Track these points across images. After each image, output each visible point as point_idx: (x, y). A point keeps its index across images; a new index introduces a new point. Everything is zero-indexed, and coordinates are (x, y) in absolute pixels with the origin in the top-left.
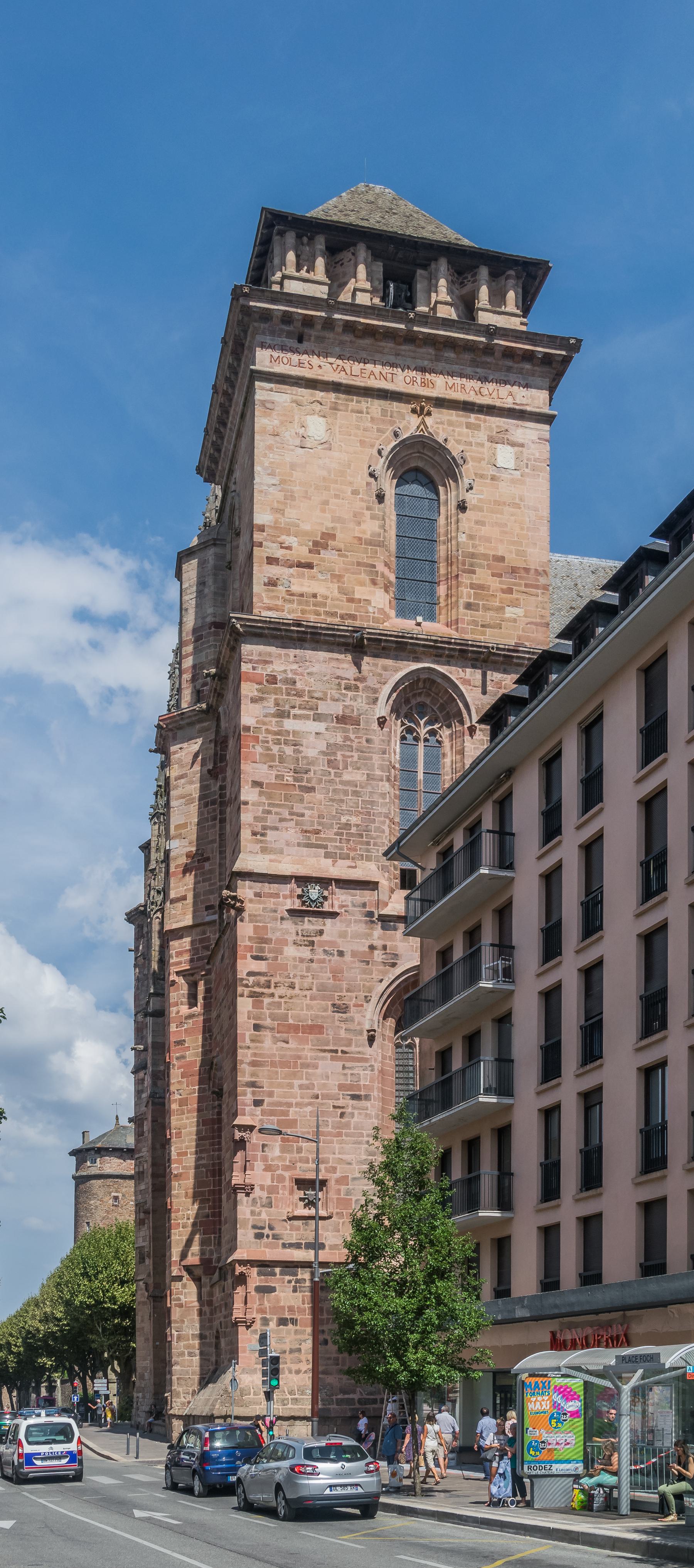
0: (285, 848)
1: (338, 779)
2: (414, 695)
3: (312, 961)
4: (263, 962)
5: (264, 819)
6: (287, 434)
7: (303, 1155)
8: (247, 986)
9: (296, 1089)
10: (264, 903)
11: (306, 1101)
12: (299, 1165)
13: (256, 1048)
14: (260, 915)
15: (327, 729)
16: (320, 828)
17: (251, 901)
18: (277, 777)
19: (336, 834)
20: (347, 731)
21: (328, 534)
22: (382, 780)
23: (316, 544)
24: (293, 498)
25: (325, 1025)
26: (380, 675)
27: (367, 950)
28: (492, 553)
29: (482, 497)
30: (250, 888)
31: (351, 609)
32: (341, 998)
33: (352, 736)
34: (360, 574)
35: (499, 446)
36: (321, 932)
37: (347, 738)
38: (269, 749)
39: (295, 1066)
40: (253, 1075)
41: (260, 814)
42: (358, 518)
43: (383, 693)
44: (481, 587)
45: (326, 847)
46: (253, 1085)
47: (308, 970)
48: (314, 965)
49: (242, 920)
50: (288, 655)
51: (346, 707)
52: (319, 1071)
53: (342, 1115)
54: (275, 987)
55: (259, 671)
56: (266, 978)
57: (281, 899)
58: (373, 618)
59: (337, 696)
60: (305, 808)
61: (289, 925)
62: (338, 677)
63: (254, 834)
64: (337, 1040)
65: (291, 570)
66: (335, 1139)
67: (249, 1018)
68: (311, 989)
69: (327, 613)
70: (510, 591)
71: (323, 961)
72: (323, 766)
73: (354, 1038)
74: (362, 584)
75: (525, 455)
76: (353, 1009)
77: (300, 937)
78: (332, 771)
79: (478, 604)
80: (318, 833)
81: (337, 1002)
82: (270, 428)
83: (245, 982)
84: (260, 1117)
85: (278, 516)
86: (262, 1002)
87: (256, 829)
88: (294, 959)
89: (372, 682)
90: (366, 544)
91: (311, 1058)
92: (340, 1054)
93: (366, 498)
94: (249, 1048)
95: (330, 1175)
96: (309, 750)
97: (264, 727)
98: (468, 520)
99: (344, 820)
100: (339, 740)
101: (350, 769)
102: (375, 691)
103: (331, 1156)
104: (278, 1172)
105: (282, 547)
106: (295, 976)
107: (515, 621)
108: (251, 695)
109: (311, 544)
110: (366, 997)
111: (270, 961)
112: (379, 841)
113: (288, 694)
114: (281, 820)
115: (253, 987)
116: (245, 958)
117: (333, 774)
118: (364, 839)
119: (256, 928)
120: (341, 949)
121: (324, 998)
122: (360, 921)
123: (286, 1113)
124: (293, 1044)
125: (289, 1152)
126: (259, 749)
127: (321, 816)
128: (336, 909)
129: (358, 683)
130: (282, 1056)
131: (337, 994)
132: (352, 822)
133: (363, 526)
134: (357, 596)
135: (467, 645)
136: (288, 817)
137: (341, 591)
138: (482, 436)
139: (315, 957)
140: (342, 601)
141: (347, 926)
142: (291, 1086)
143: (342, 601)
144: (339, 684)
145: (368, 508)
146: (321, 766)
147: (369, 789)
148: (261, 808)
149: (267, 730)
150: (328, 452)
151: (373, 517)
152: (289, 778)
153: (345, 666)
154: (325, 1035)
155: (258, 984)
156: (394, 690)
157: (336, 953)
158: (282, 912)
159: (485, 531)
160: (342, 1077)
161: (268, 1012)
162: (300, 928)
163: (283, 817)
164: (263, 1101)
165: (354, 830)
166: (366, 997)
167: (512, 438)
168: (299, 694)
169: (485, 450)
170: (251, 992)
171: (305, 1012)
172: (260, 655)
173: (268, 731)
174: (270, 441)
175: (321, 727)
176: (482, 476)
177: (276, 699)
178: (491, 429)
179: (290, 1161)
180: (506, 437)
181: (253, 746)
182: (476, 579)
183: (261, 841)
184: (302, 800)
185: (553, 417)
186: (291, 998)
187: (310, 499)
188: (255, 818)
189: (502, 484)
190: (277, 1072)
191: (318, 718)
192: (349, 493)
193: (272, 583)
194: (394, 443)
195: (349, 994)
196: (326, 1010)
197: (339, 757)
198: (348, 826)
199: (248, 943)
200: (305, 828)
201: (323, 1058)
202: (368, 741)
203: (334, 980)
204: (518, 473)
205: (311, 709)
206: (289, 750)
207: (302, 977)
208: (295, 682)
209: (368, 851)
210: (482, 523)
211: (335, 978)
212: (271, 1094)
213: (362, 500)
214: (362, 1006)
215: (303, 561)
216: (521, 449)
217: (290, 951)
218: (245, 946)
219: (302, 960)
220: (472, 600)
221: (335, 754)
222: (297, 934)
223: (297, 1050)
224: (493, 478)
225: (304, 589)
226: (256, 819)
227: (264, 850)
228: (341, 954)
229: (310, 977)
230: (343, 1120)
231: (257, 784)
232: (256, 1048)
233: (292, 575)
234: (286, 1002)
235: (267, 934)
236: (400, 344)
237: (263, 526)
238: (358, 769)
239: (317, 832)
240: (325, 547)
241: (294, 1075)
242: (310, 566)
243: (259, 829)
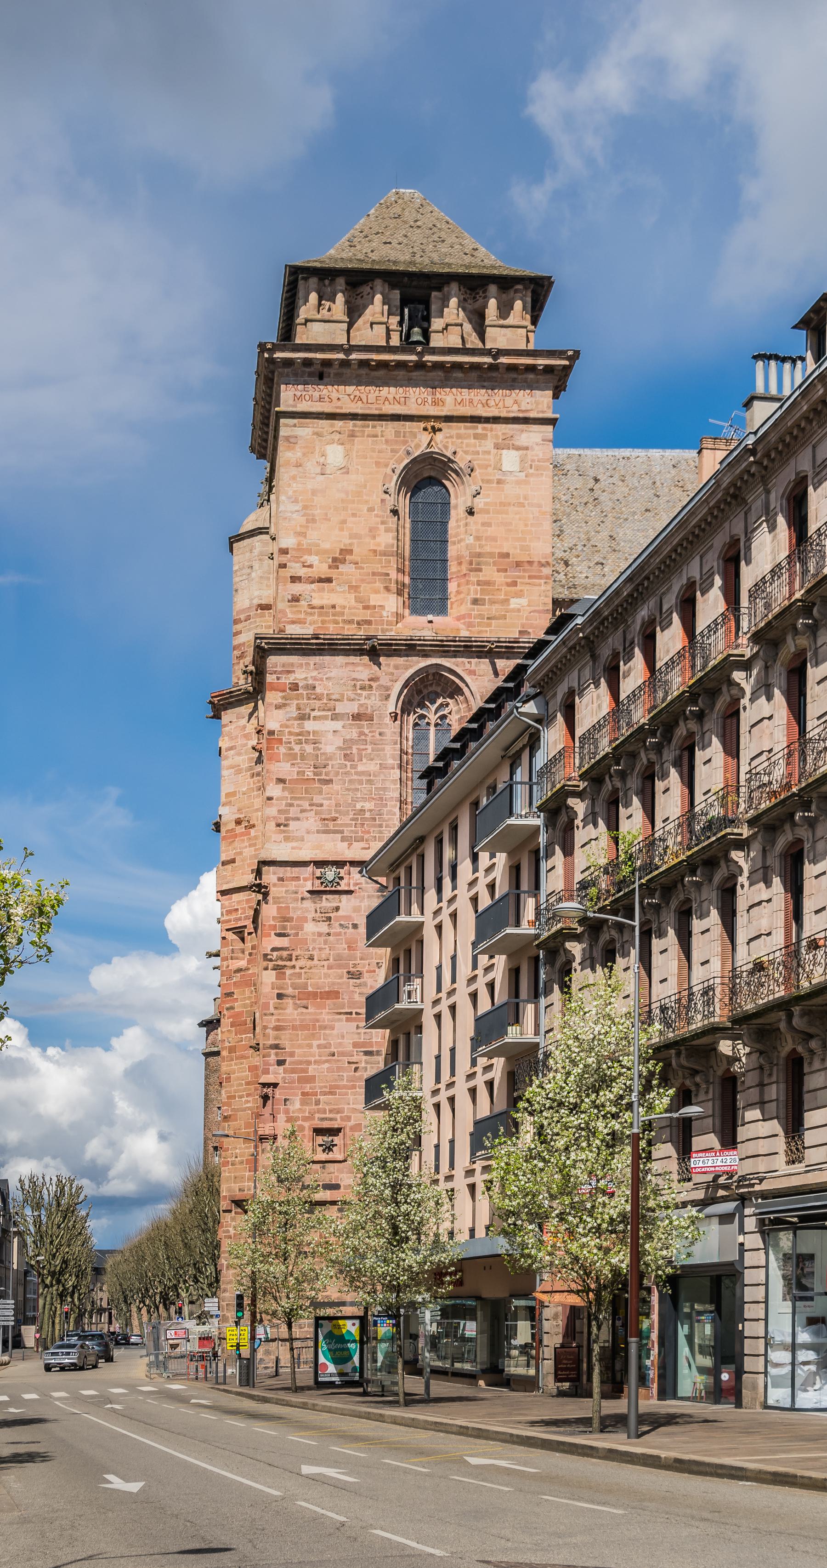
0: (306, 836)
1: (353, 771)
2: (426, 687)
3: (329, 934)
5: (288, 812)
6: (309, 464)
7: (320, 1106)
8: (271, 960)
9: (315, 1049)
10: (287, 886)
11: (324, 1058)
12: (317, 1116)
13: (279, 1014)
14: (282, 897)
15: (343, 727)
16: (337, 815)
17: (275, 885)
18: (298, 773)
19: (352, 819)
20: (362, 726)
21: (346, 550)
22: (393, 768)
23: (335, 560)
24: (314, 521)
26: (392, 674)
28: (497, 551)
29: (488, 500)
30: (274, 873)
31: (367, 615)
32: (355, 965)
33: (366, 731)
34: (375, 582)
35: (505, 452)
36: (337, 909)
37: (362, 733)
38: (291, 749)
39: (314, 1029)
40: (276, 1038)
41: (283, 807)
42: (373, 532)
43: (394, 690)
44: (488, 583)
45: (342, 832)
46: (276, 1047)
47: (325, 942)
48: (331, 938)
49: (266, 903)
50: (309, 664)
51: (361, 705)
52: (335, 1032)
53: (356, 1069)
54: (296, 959)
55: (282, 681)
56: (288, 952)
57: (302, 882)
58: (387, 621)
59: (353, 696)
60: (324, 799)
61: (308, 904)
62: (354, 679)
63: (278, 825)
65: (313, 586)
66: (350, 1091)
67: (273, 989)
69: (344, 621)
70: (514, 584)
71: (339, 934)
72: (340, 759)
74: (377, 592)
75: (529, 457)
76: (366, 975)
77: (318, 914)
78: (348, 764)
79: (485, 599)
80: (335, 820)
81: (351, 969)
82: (293, 460)
83: (269, 957)
84: (283, 1075)
85: (301, 538)
86: (284, 973)
87: (280, 821)
88: (313, 934)
89: (384, 681)
90: (380, 555)
91: (328, 1020)
92: (354, 1015)
93: (381, 513)
95: (345, 1123)
96: (328, 747)
97: (287, 730)
98: (476, 523)
99: (358, 806)
100: (355, 735)
101: (364, 760)
102: (387, 689)
103: (346, 1107)
104: (298, 1123)
105: (304, 566)
106: (314, 949)
107: (519, 610)
108: (275, 702)
109: (330, 560)
110: (378, 963)
111: (292, 937)
112: (390, 823)
113: (309, 699)
114: (302, 811)
115: (276, 961)
116: (270, 935)
117: (349, 767)
118: (377, 822)
119: (279, 908)
121: (340, 967)
122: (373, 896)
123: (306, 1071)
125: (307, 1104)
126: (282, 750)
127: (338, 805)
128: (352, 888)
129: (372, 683)
130: (302, 1021)
131: (351, 962)
132: (366, 808)
133: (378, 539)
134: (372, 603)
135: (471, 641)
136: (309, 808)
137: (358, 600)
138: (489, 444)
139: (332, 931)
140: (359, 609)
141: (360, 902)
142: (310, 1046)
143: (359, 609)
144: (355, 685)
145: (383, 523)
146: (339, 760)
147: (382, 777)
148: (284, 802)
149: (289, 732)
150: (346, 475)
151: (387, 530)
152: (309, 774)
153: (360, 668)
155: (281, 959)
156: (405, 686)
157: (350, 926)
158: (302, 893)
159: (490, 531)
160: (357, 1036)
161: (289, 982)
162: (318, 906)
163: (304, 808)
164: (285, 1061)
165: (367, 815)
166: (378, 963)
167: (517, 443)
168: (318, 698)
169: (491, 457)
172: (283, 666)
173: (290, 733)
174: (294, 471)
175: (338, 725)
176: (489, 481)
177: (297, 704)
178: (497, 436)
179: (309, 1113)
180: (511, 442)
181: (278, 748)
182: (482, 577)
183: (284, 831)
184: (320, 793)
185: (556, 420)
186: (311, 968)
187: (329, 520)
188: (279, 811)
189: (506, 486)
190: (298, 1035)
191: (335, 717)
192: (365, 511)
193: (295, 599)
194: (406, 461)
196: (341, 977)
197: (355, 751)
198: (362, 811)
199: (272, 923)
200: (323, 817)
201: (340, 1020)
202: (380, 734)
203: (349, 950)
204: (523, 474)
205: (329, 710)
206: (309, 748)
207: (320, 949)
208: (315, 687)
209: (381, 832)
210: (489, 525)
211: (350, 948)
212: (292, 1054)
213: (377, 516)
215: (323, 577)
216: (525, 452)
217: (310, 928)
218: (270, 925)
219: (320, 934)
220: (478, 596)
221: (351, 748)
222: (316, 911)
223: (315, 1014)
224: (499, 482)
225: (325, 602)
226: (280, 811)
227: (287, 839)
229: (328, 949)
230: (357, 1074)
231: (281, 781)
232: (279, 1014)
233: (313, 590)
236: (411, 371)
237: (288, 549)
238: (372, 760)
239: (335, 819)
240: (343, 561)
241: (313, 1036)
242: (329, 580)
243: (283, 821)
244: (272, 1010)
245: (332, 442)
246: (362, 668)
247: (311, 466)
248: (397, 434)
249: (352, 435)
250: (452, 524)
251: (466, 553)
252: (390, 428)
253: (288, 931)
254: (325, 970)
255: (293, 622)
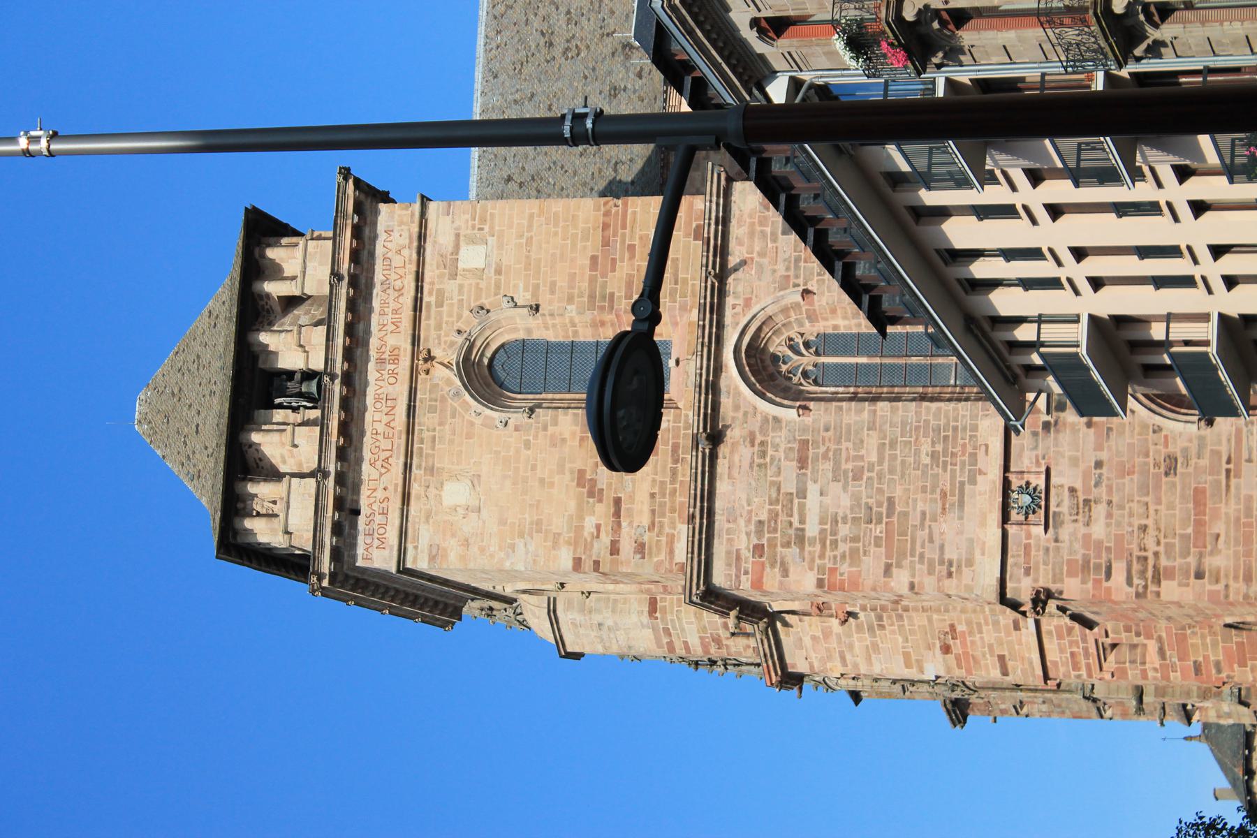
1: (877, 468)
2: (765, 368)
3: (1110, 503)
4: (1114, 566)
8: (1146, 587)
10: (1037, 563)
14: (1053, 569)
15: (815, 482)
16: (938, 491)
17: (1036, 580)
18: (877, 545)
19: (945, 470)
21: (579, 479)
22: (875, 411)
23: (591, 494)
24: (539, 523)
25: (1193, 486)
26: (746, 414)
27: (1092, 430)
29: (521, 285)
30: (1019, 581)
32: (1156, 465)
33: (822, 449)
35: (461, 265)
36: (1072, 490)
37: (825, 456)
38: (843, 556)
41: (925, 567)
45: (962, 484)
47: (1121, 507)
48: (1115, 500)
50: (728, 530)
51: (787, 458)
54: (1145, 550)
55: (749, 566)
57: (1032, 541)
58: (675, 422)
59: (774, 469)
60: (914, 509)
61: (1065, 532)
62: (751, 467)
63: (950, 575)
64: (1214, 471)
65: (624, 524)
67: (1188, 585)
68: (1147, 504)
69: (673, 481)
71: (1110, 488)
72: (860, 486)
73: (1209, 448)
75: (469, 232)
76: (1171, 449)
77: (1080, 517)
78: (866, 475)
80: (945, 494)
81: (1162, 470)
83: (1141, 590)
85: (561, 540)
86: (1166, 568)
87: (945, 573)
88: (1108, 525)
91: (1238, 503)
92: (1231, 466)
93: (533, 432)
94: (1227, 586)
96: (842, 503)
98: (551, 302)
99: (926, 460)
101: (863, 452)
105: (598, 536)
106: (1130, 525)
108: (778, 577)
109: (591, 500)
110: (1154, 432)
111: (1112, 556)
113: (775, 530)
114: (931, 540)
115: (1146, 580)
116: (1108, 590)
117: (870, 474)
120: (1093, 464)
121: (1158, 487)
122: (1056, 439)
124: (1219, 528)
126: (845, 568)
127: (924, 489)
128: (1043, 469)
129: (757, 442)
130: (1237, 543)
132: (930, 449)
133: (567, 435)
136: (927, 531)
138: (451, 287)
139: (1105, 498)
140: (657, 461)
144: (759, 466)
145: (545, 428)
146: (862, 487)
148: (918, 566)
151: (555, 423)
152: (879, 530)
153: (736, 458)
154: (1207, 486)
155: (1143, 573)
156: (762, 396)
157: (1098, 471)
159: (562, 283)
162: (1067, 518)
163: (927, 538)
165: (939, 448)
167: (450, 249)
168: (774, 516)
169: (466, 283)
170: (1153, 582)
171: (1177, 512)
172: (729, 565)
173: (822, 556)
175: (813, 490)
176: (498, 286)
177: (783, 546)
180: (449, 257)
181: (842, 574)
184: (906, 514)
185: (423, 197)
186: (1159, 529)
191: (802, 494)
192: (529, 452)
193: (641, 548)
195: (1151, 454)
196: (1174, 485)
197: (850, 466)
198: (934, 455)
199: (1090, 585)
200: (939, 510)
201: (1238, 488)
202: (827, 430)
204: (490, 239)
205: (791, 501)
206: (844, 530)
207: (1131, 515)
208: (760, 522)
209: (964, 429)
210: (553, 284)
213: (536, 437)
214: (1166, 437)
215: (612, 510)
216: (462, 238)
217: (1098, 530)
218: (1094, 588)
219: (1109, 515)
221: (846, 472)
222: (1076, 521)
223: (1227, 523)
224: (498, 272)
225: (646, 509)
226: (931, 572)
227: (970, 563)
228: (1099, 464)
229: (1131, 504)
231: (888, 570)
232: (1227, 576)
233: (631, 523)
234: (1165, 537)
235: (1077, 561)
237: (574, 559)
238: (862, 441)
242: (618, 502)
244: (1220, 587)
245: (439, 498)
246: (734, 455)
247: (468, 526)
248: (432, 410)
249: (431, 470)
250: (551, 336)
251: (588, 316)
252: (424, 419)
253: (1103, 561)
254: (1162, 508)
255: (671, 552)
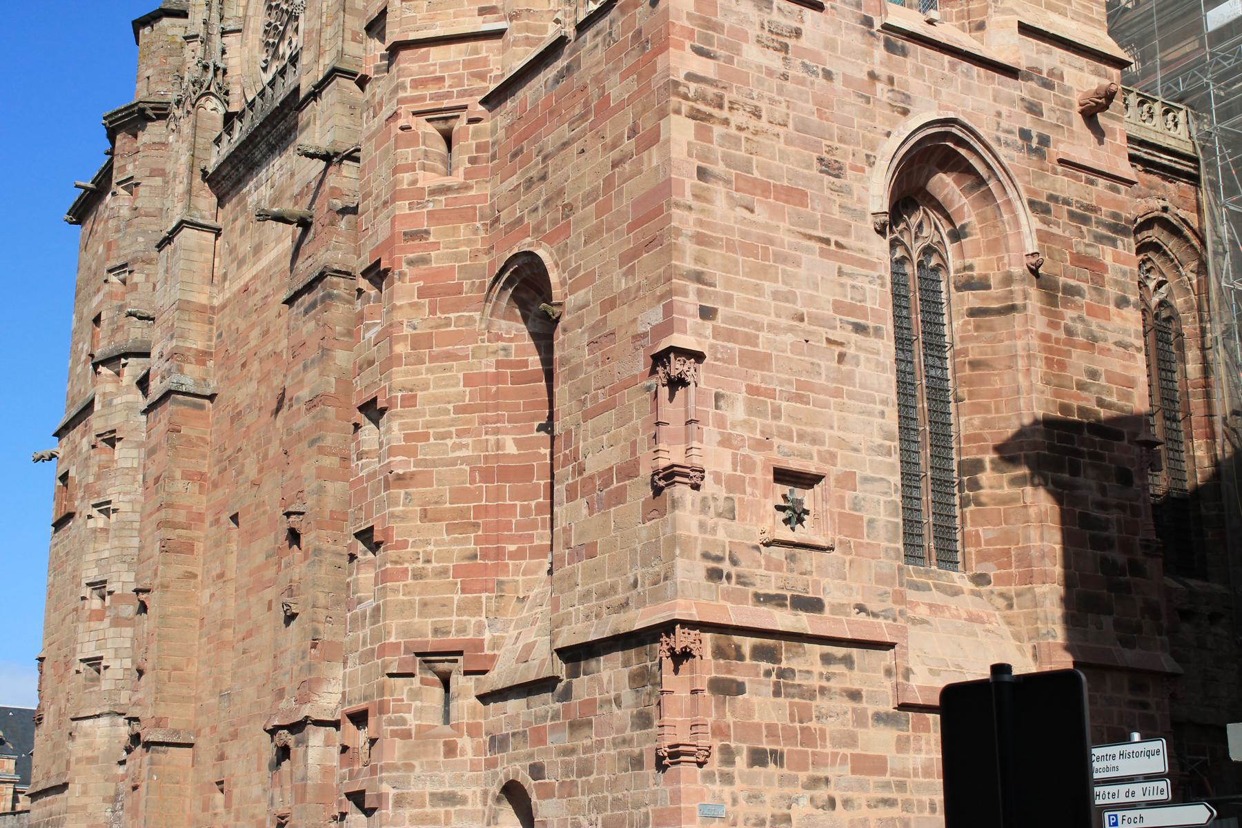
4: (711, 62)
8: (686, 97)
9: (767, 299)
25: (809, 191)
27: (866, 78)
32: (831, 150)
39: (765, 258)
48: (789, 85)
56: (716, 91)
64: (828, 222)
66: (832, 400)
67: (690, 155)
68: (785, 125)
71: (801, 82)
73: (853, 223)
76: (849, 173)
77: (766, 34)
81: (825, 156)
83: (682, 89)
86: (710, 130)
88: (759, 67)
91: (790, 246)
94: (690, 208)
103: (827, 432)
104: (741, 452)
110: (868, 156)
115: (695, 101)
120: (828, 68)
121: (806, 145)
122: (854, 28)
123: (751, 340)
124: (761, 215)
125: (761, 414)
130: (745, 234)
131: (824, 142)
154: (809, 209)
155: (702, 97)
160: (838, 290)
162: (767, 18)
170: (692, 108)
171: (777, 162)
179: (762, 433)
186: (756, 133)
195: (842, 145)
196: (809, 167)
199: (687, 24)
201: (809, 250)
203: (820, 117)
207: (772, 101)
211: (820, 113)
212: (728, 300)
214: (863, 170)
217: (752, 54)
219: (770, 73)
222: (762, 27)
223: (766, 226)
228: (828, 75)
229: (784, 104)
232: (703, 211)
234: (747, 139)
235: (716, 15)
241: (763, 272)
244: (688, 199)
253: (713, 49)
254: (781, 144)
